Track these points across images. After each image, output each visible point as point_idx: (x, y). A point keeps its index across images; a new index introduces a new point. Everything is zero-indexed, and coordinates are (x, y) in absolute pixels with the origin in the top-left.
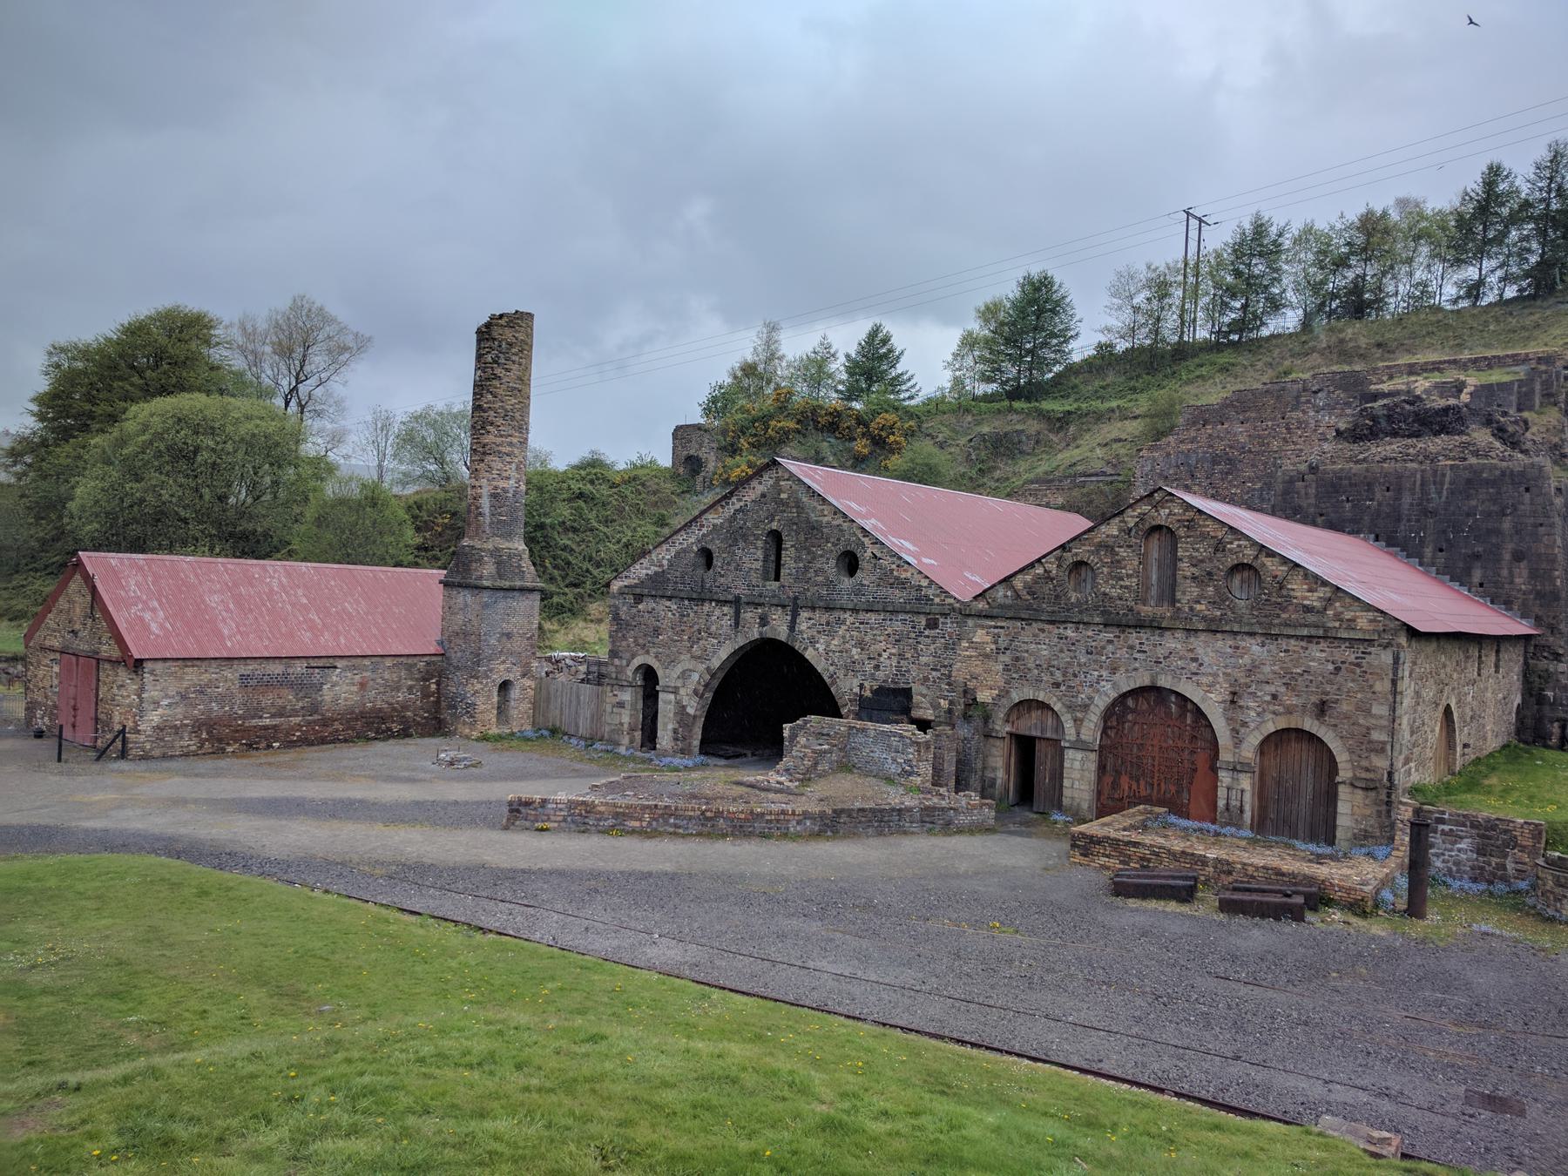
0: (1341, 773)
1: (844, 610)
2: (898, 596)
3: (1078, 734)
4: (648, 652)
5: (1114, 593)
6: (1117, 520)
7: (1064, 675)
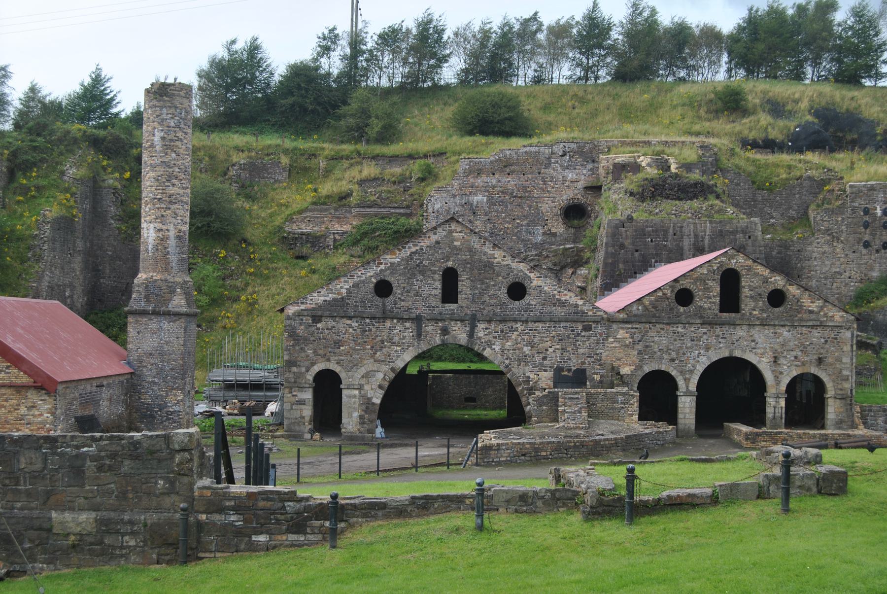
0: (829, 393)
1: (516, 321)
2: (560, 312)
3: (687, 387)
4: (329, 360)
5: (706, 306)
6: (707, 265)
7: (677, 354)
